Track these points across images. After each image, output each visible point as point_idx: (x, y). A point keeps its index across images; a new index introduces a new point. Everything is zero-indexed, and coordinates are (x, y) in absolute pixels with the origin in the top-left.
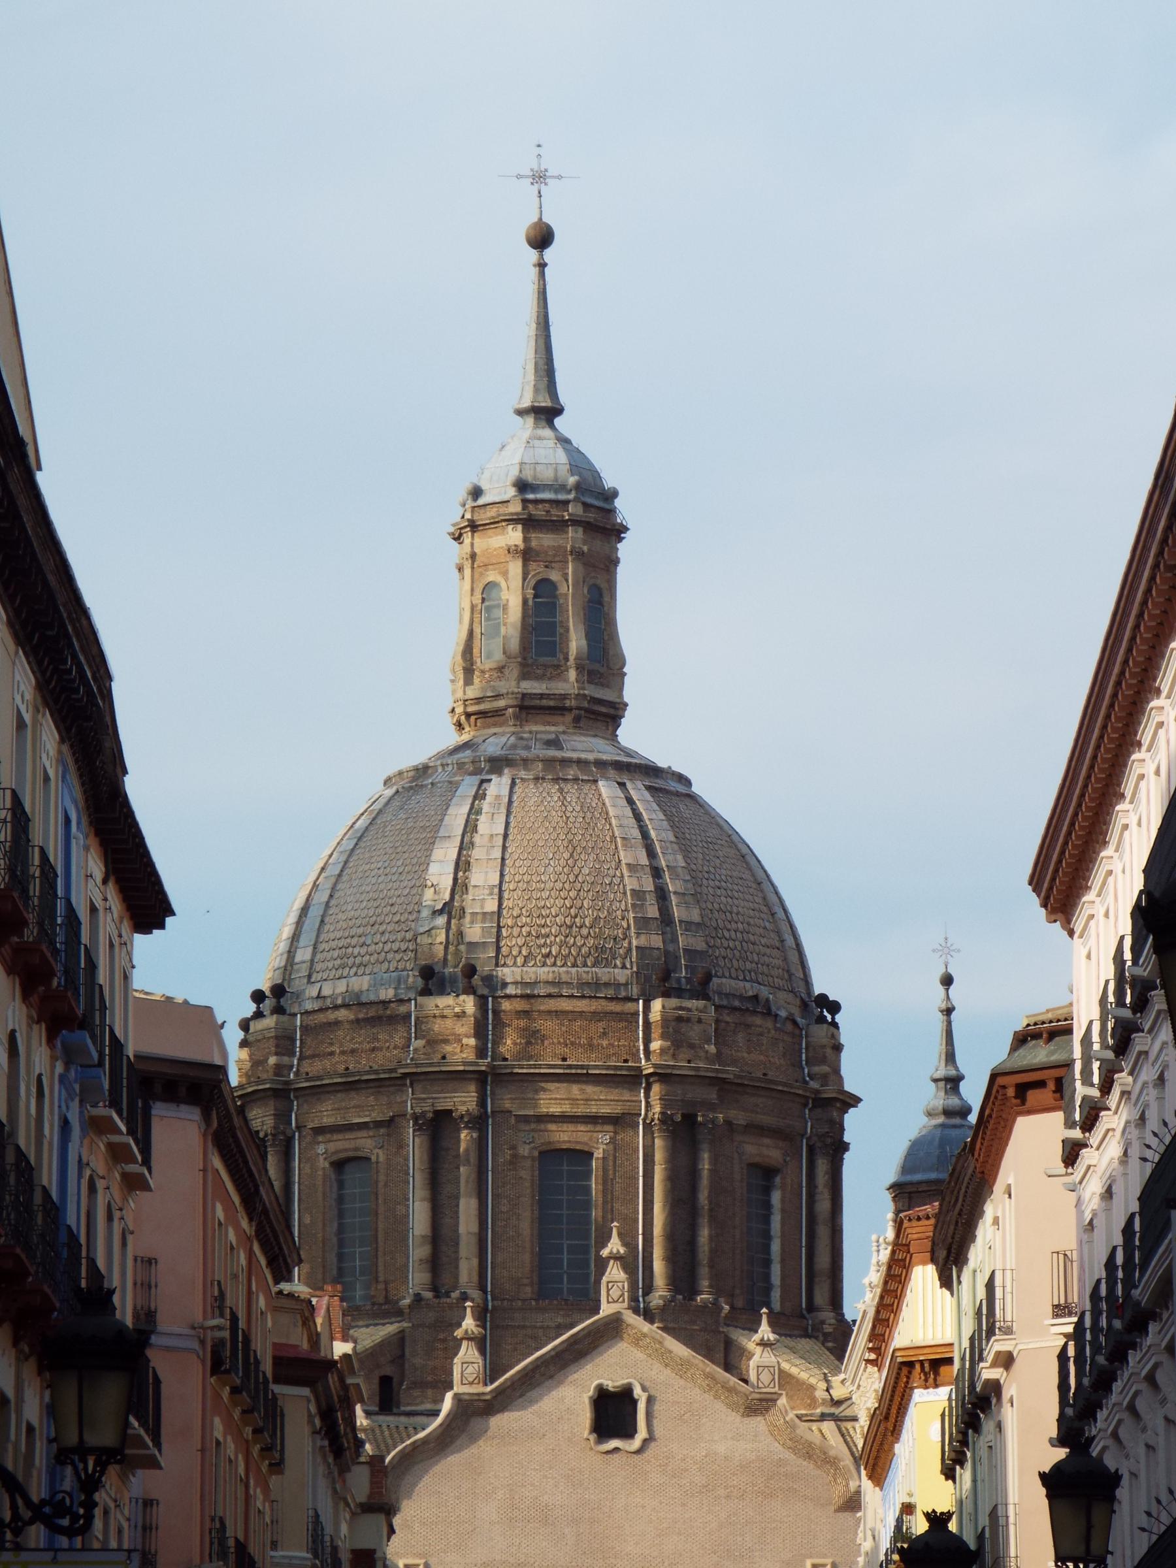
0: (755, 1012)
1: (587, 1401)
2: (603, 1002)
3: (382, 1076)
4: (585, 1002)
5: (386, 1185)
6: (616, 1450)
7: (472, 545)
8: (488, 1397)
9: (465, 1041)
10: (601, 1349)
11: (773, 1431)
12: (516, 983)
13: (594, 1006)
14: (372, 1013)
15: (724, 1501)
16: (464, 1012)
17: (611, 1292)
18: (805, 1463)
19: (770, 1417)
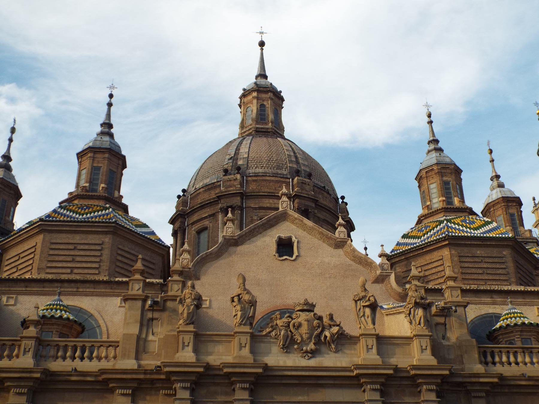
0: (324, 191)
1: (274, 241)
2: (279, 178)
3: (212, 201)
4: (274, 178)
5: (212, 233)
6: (286, 259)
7: (244, 100)
8: (236, 238)
9: (237, 186)
10: (279, 224)
11: (346, 254)
12: (253, 173)
13: (277, 179)
14: (210, 187)
15: (328, 279)
16: (237, 178)
17: (283, 205)
18: (359, 266)
19: (344, 249)
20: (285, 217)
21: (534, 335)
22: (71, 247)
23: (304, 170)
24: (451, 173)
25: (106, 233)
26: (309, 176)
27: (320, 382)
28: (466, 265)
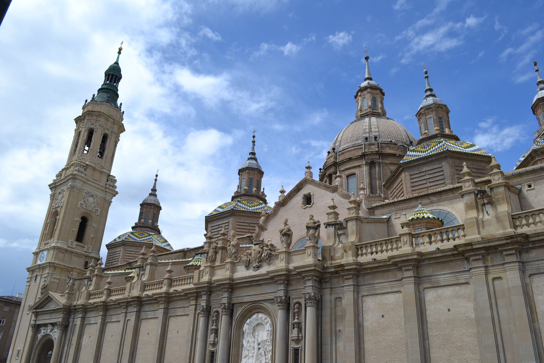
13: (355, 148)
20: (306, 182)
21: (423, 225)
22: (218, 227)
23: (374, 135)
24: (432, 111)
25: (230, 216)
26: (376, 138)
27: (259, 283)
28: (415, 180)
